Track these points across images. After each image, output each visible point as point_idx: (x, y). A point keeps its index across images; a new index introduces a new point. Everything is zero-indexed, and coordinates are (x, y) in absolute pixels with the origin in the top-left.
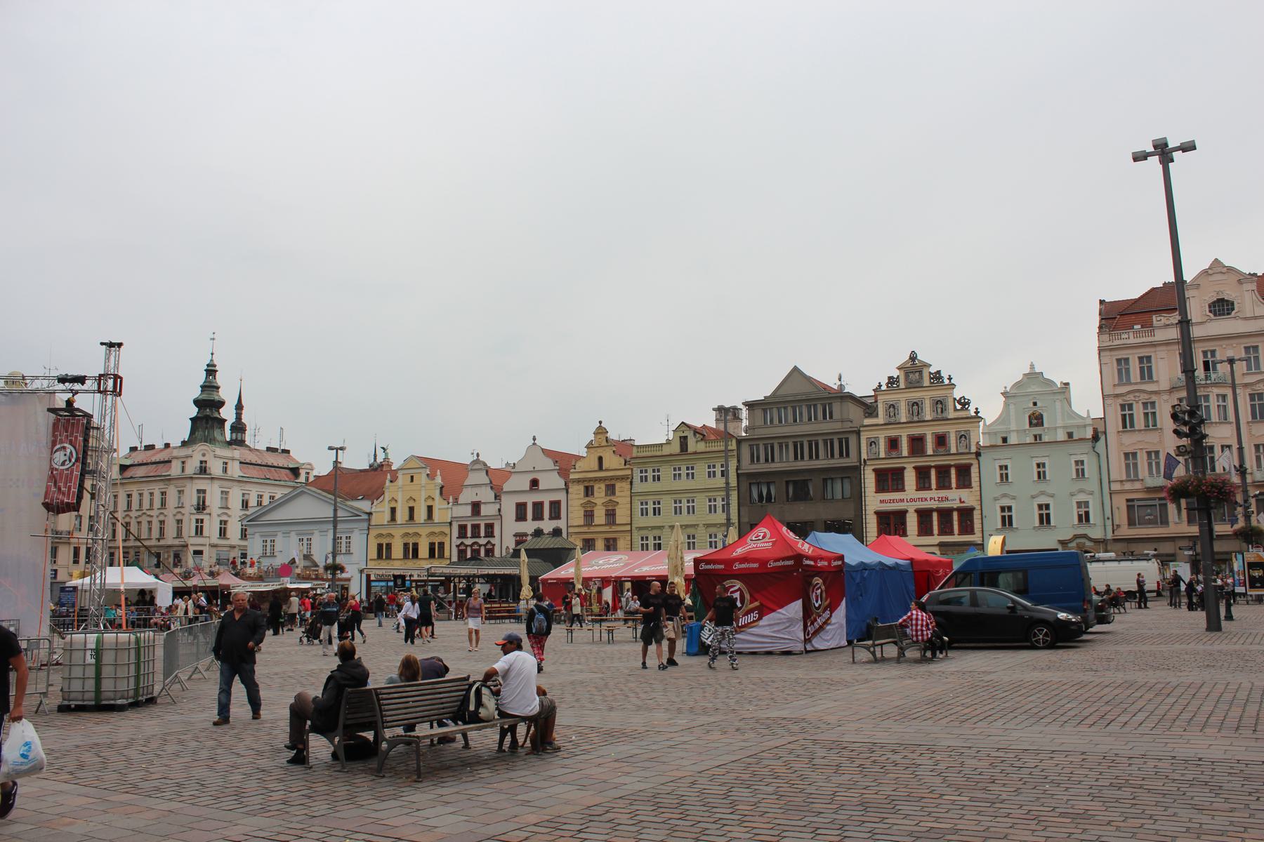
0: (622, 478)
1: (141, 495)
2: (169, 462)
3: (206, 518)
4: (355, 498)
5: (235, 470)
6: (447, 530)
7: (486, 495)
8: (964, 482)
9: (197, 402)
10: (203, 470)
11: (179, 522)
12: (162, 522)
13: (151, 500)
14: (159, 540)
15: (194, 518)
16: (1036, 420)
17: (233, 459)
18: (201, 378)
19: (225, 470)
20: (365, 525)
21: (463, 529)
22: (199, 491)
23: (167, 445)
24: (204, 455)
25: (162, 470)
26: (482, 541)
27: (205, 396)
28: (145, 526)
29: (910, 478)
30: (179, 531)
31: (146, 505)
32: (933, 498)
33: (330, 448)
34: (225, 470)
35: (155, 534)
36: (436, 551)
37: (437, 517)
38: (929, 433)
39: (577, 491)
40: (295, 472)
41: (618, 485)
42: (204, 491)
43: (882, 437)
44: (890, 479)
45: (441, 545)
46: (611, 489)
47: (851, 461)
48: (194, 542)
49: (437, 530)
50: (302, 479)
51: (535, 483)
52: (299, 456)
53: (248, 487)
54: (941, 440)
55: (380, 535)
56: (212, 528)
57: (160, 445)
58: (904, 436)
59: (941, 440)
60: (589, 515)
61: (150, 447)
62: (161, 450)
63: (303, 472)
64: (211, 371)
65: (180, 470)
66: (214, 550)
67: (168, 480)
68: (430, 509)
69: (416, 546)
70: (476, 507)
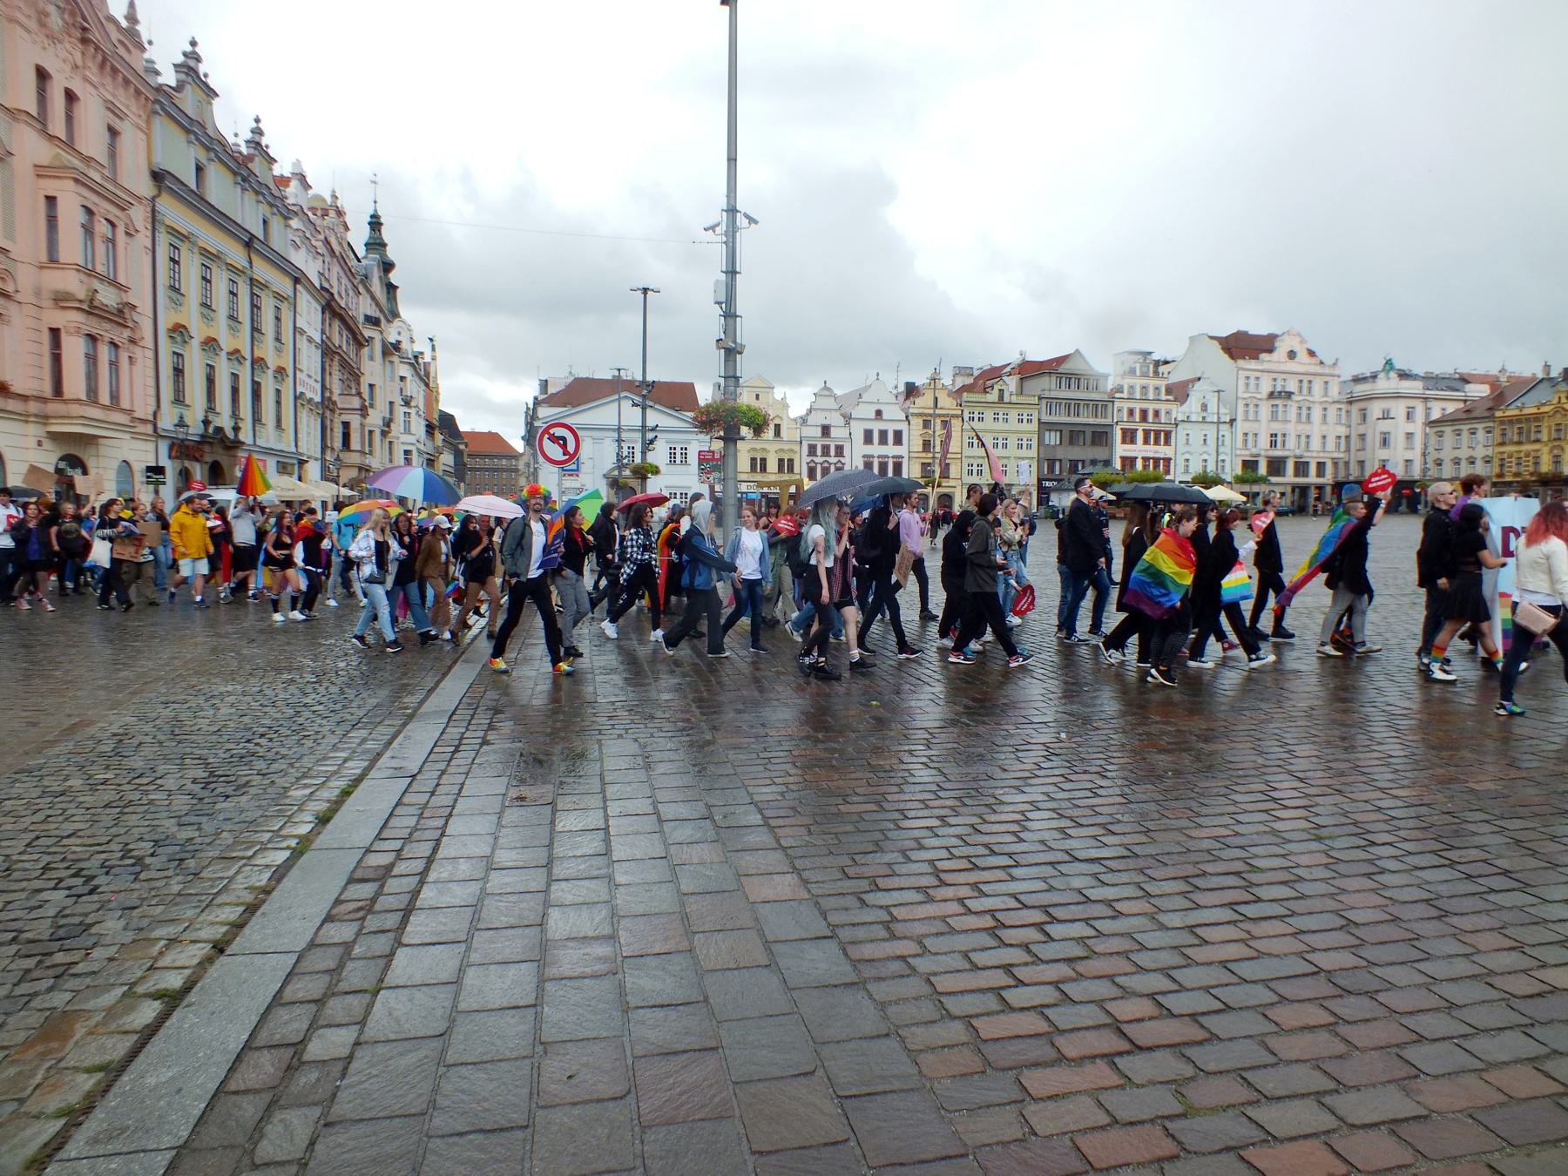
0: (957, 416)
6: (796, 448)
7: (835, 420)
8: (1167, 443)
16: (1204, 407)
21: (812, 450)
26: (833, 460)
29: (1140, 436)
32: (1152, 450)
36: (786, 465)
38: (1151, 407)
39: (917, 423)
41: (954, 421)
43: (1126, 406)
44: (1129, 437)
45: (791, 461)
46: (945, 424)
47: (1108, 421)
49: (786, 447)
51: (879, 413)
54: (1157, 413)
58: (1138, 406)
59: (1157, 413)
60: (927, 445)
69: (764, 461)
70: (826, 430)
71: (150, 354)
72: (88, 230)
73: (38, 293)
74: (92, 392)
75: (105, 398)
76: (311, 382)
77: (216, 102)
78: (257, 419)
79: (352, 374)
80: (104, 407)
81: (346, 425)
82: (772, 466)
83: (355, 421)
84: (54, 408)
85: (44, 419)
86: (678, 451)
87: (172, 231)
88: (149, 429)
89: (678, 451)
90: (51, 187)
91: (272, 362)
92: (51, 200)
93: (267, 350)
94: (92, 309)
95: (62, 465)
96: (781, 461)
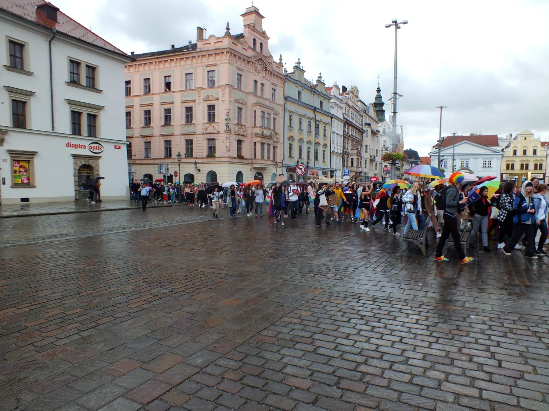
4: (490, 146)
20: (500, 156)
37: (538, 153)
49: (539, 159)
55: (508, 160)
68: (535, 152)
71: (282, 145)
72: (263, 117)
73: (252, 134)
74: (263, 157)
75: (266, 158)
76: (339, 147)
77: (305, 74)
78: (316, 159)
79: (358, 143)
80: (265, 160)
81: (352, 159)
82: (531, 166)
83: (355, 157)
84: (254, 161)
85: (252, 164)
86: (487, 162)
87: (290, 111)
88: (281, 164)
89: (487, 162)
90: (255, 108)
91: (322, 143)
92: (255, 111)
93: (321, 140)
94: (263, 136)
95: (257, 175)
96: (536, 165)
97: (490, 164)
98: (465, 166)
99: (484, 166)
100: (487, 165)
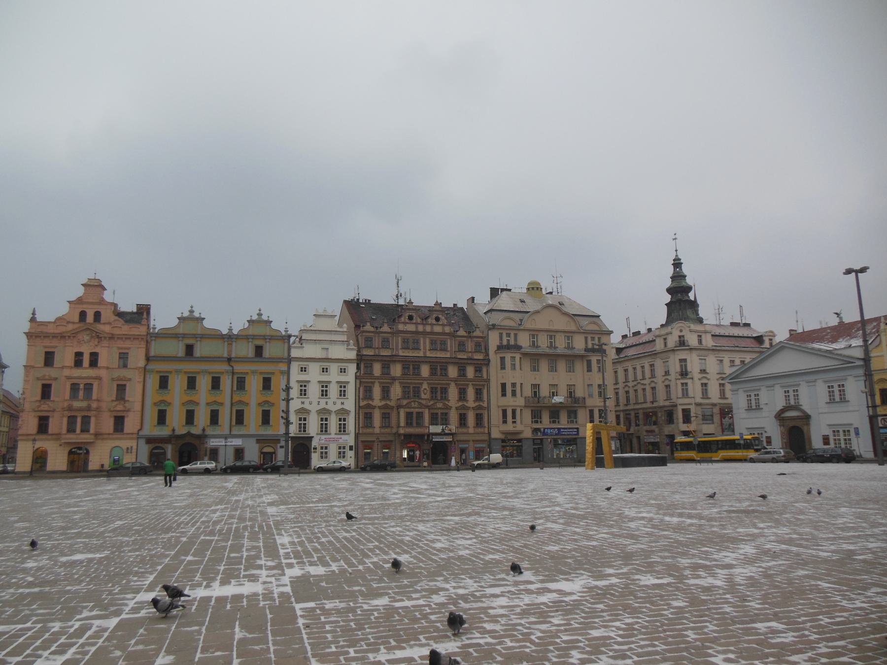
1: (635, 369)
2: (654, 341)
3: (689, 382)
5: (708, 341)
9: (669, 290)
10: (682, 342)
11: (668, 386)
12: (653, 388)
13: (643, 372)
14: (652, 402)
15: (679, 382)
17: (706, 332)
18: (670, 271)
19: (700, 342)
22: (681, 360)
23: (650, 330)
24: (681, 331)
25: (648, 348)
27: (675, 285)
28: (640, 392)
30: (668, 392)
31: (639, 376)
33: (849, 272)
34: (700, 342)
35: (649, 398)
40: (759, 339)
42: (685, 360)
48: (682, 403)
50: (767, 344)
52: (759, 327)
53: (722, 354)
56: (695, 389)
57: (643, 331)
61: (637, 334)
62: (646, 334)
63: (766, 340)
64: (677, 264)
65: (662, 346)
66: (699, 408)
67: (654, 354)
97: (842, 392)
98: (792, 402)
99: (832, 401)
100: (837, 397)
